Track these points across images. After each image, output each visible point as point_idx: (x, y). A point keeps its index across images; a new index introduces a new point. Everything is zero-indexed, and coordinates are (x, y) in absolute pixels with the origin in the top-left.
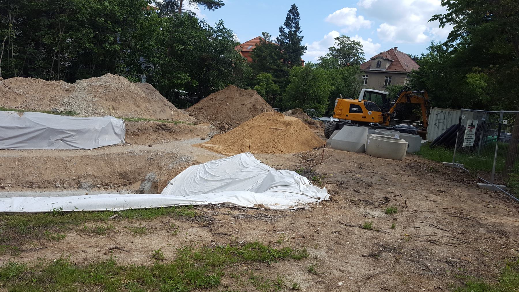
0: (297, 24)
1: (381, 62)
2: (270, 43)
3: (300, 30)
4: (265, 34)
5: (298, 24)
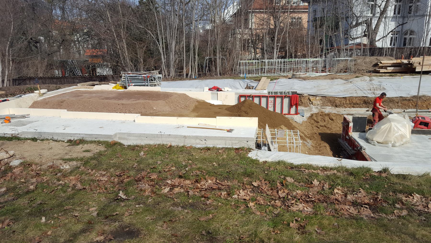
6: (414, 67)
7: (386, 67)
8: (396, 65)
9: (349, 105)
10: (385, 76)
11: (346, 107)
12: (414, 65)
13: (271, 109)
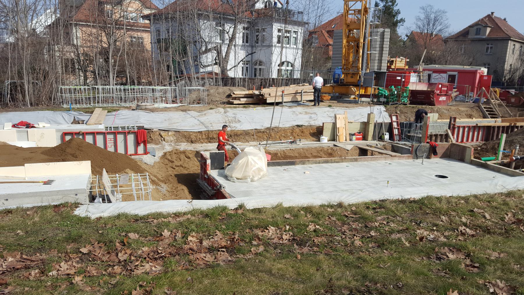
1: (480, 29)
3: (396, 4)
6: (265, 98)
7: (239, 98)
8: (249, 96)
9: (206, 140)
10: (239, 107)
11: (203, 143)
12: (265, 96)
13: (111, 149)
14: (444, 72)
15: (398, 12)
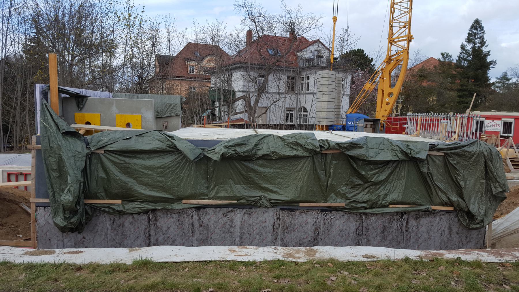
0: (482, 38)
2: (450, 63)
3: (486, 45)
4: (444, 54)
5: (483, 39)
14: (499, 118)
15: (488, 54)
